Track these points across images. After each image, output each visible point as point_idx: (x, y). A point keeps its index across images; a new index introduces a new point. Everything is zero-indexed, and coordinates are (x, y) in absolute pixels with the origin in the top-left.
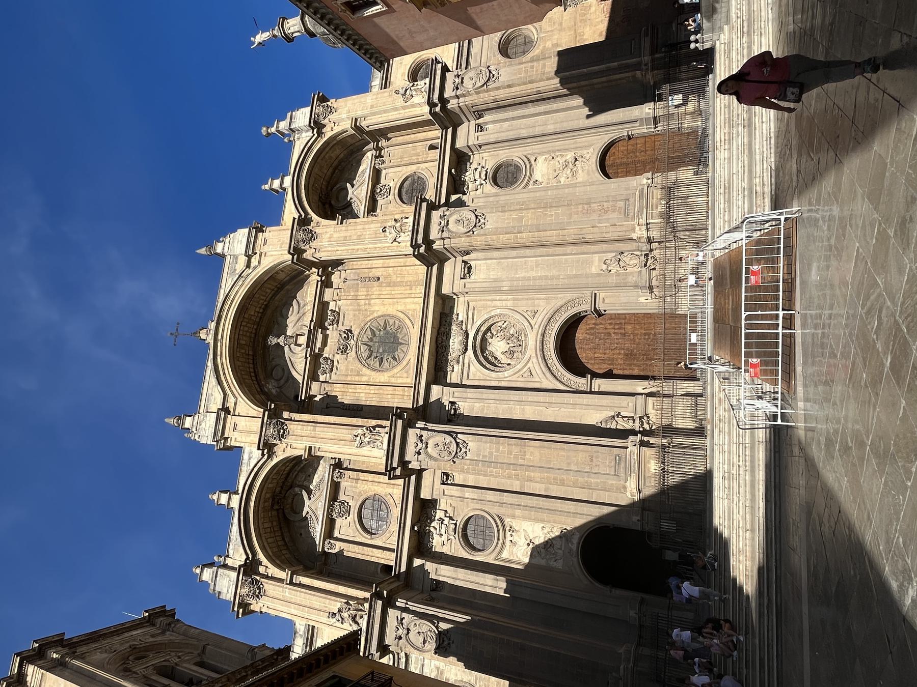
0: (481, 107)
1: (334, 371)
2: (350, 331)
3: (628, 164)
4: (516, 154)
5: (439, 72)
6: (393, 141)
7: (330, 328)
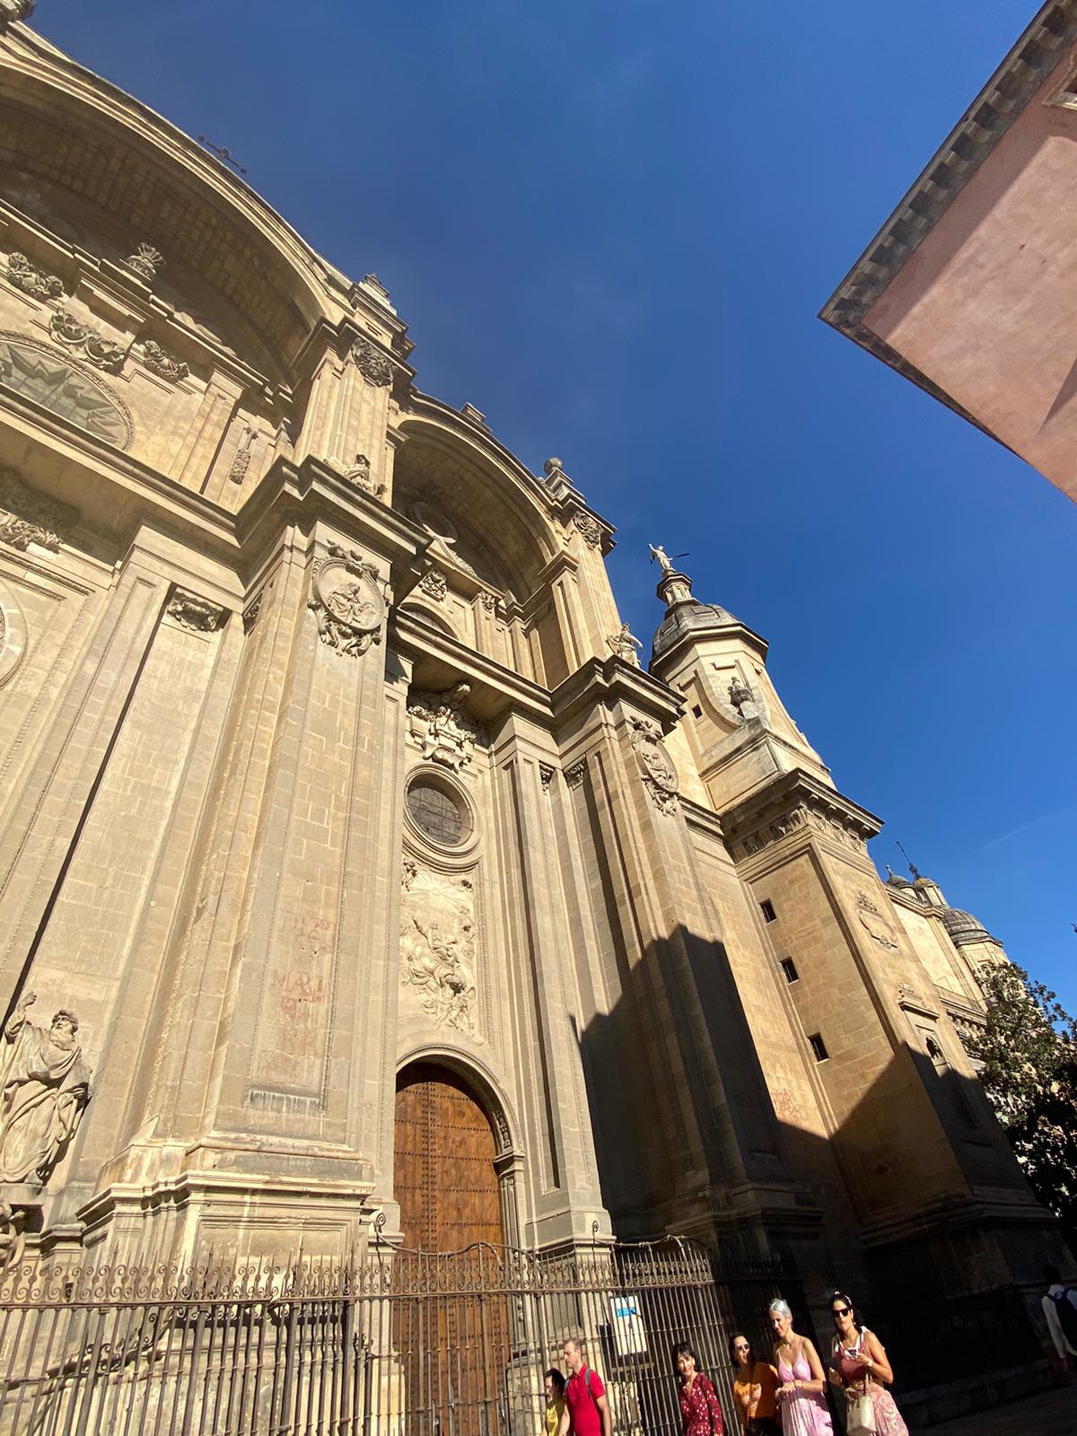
0: (595, 775)
1: (8, 285)
2: (116, 370)
3: (425, 1156)
4: (483, 843)
6: (522, 642)
7: (142, 348)
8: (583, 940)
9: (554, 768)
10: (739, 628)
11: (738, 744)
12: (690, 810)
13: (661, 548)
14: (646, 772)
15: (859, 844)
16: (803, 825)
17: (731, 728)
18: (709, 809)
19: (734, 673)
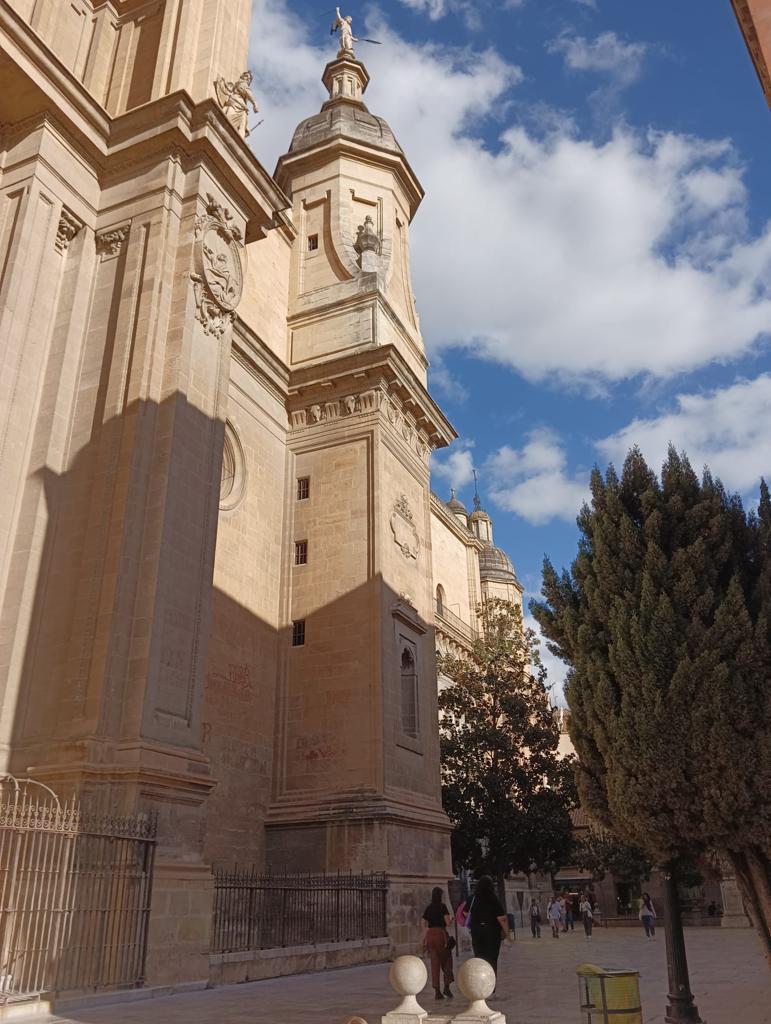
0: (135, 251)
5: (258, 198)
8: (46, 446)
9: (84, 224)
10: (398, 159)
11: (343, 296)
12: (240, 333)
13: (350, 19)
14: (200, 270)
15: (424, 450)
16: (374, 409)
17: (343, 275)
18: (284, 362)
19: (372, 212)
